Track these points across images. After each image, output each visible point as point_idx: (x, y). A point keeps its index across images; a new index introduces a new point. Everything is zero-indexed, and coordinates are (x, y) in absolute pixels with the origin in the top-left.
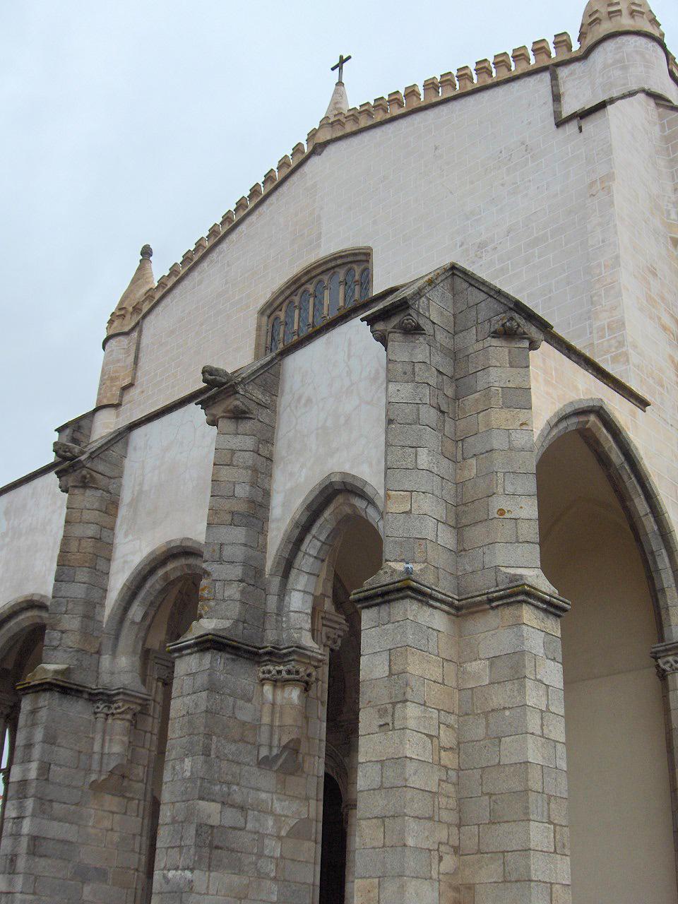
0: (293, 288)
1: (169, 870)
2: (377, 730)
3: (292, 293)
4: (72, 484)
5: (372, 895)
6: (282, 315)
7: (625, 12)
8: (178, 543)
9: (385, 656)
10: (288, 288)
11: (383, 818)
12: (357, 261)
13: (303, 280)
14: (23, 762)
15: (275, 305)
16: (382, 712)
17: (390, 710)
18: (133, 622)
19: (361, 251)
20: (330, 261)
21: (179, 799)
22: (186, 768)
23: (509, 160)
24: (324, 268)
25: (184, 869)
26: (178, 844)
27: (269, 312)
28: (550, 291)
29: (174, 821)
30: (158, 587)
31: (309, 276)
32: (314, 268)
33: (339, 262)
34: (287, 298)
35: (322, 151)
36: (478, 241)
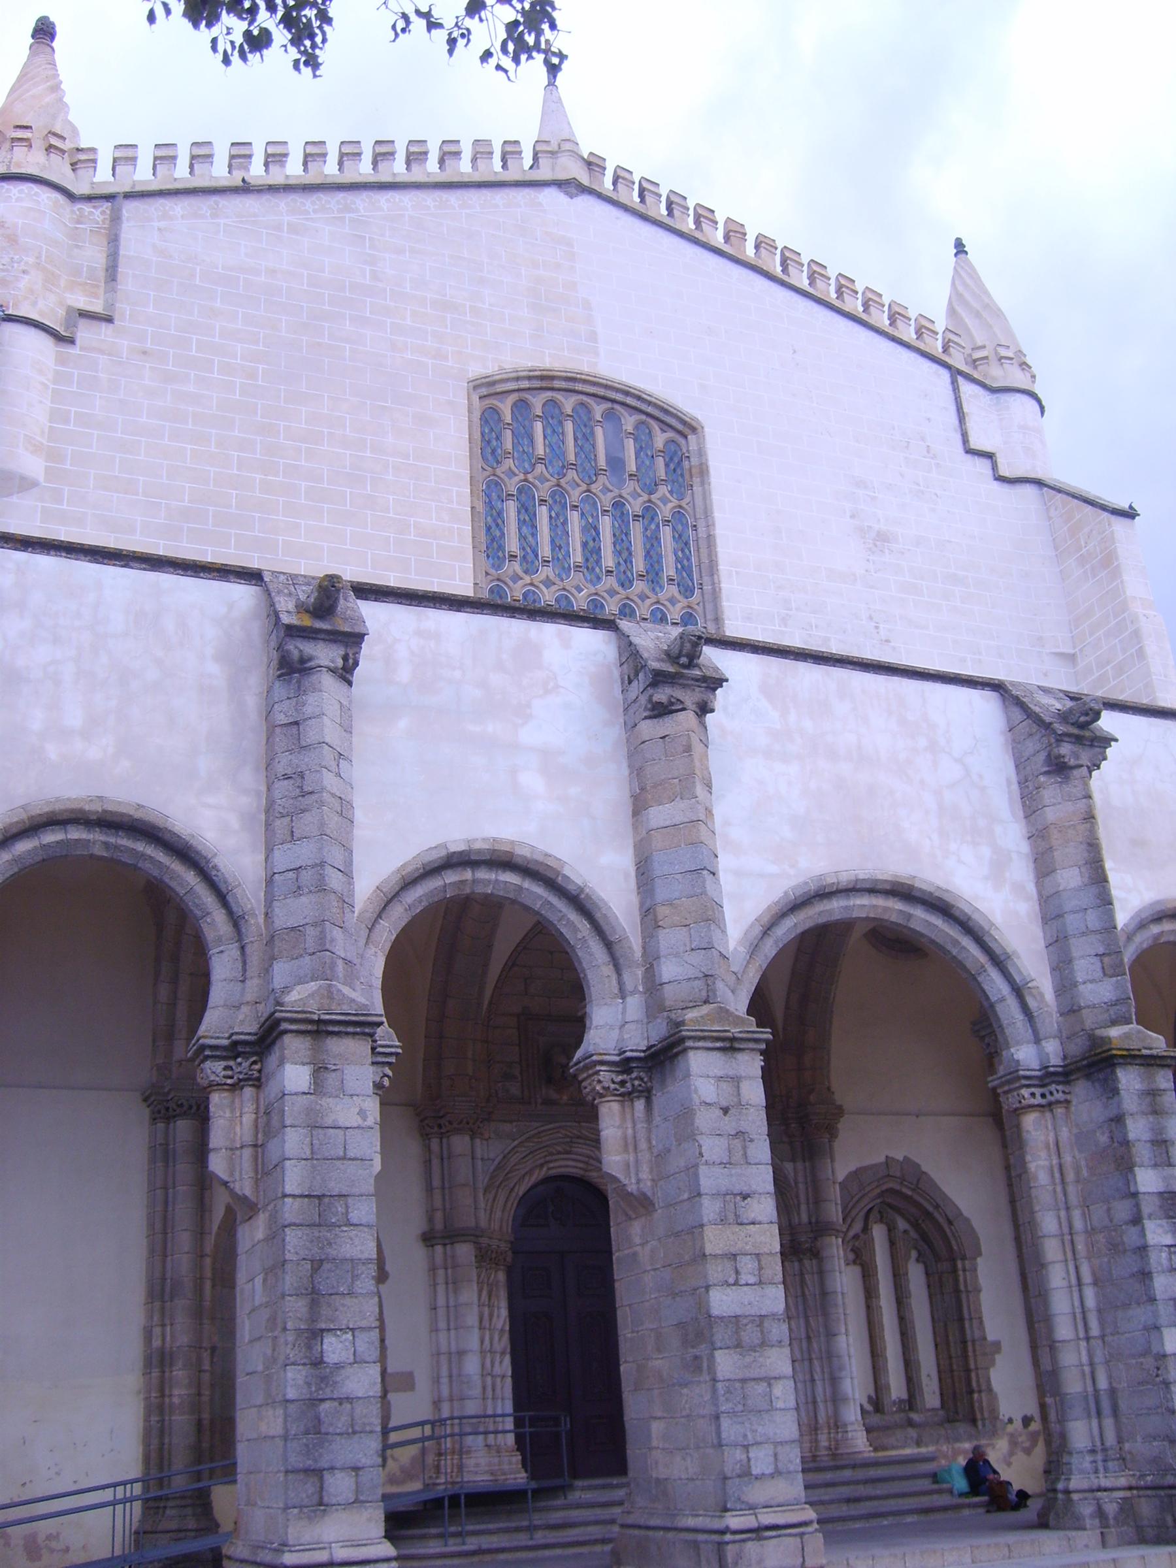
0: (537, 384)
3: (529, 389)
6: (506, 409)
7: (992, 357)
10: (529, 378)
12: (662, 422)
13: (557, 384)
15: (500, 388)
19: (680, 414)
20: (617, 390)
23: (907, 447)
24: (601, 392)
27: (484, 391)
30: (1145, 946)
31: (570, 385)
32: (585, 382)
33: (629, 401)
34: (519, 390)
35: (577, 195)
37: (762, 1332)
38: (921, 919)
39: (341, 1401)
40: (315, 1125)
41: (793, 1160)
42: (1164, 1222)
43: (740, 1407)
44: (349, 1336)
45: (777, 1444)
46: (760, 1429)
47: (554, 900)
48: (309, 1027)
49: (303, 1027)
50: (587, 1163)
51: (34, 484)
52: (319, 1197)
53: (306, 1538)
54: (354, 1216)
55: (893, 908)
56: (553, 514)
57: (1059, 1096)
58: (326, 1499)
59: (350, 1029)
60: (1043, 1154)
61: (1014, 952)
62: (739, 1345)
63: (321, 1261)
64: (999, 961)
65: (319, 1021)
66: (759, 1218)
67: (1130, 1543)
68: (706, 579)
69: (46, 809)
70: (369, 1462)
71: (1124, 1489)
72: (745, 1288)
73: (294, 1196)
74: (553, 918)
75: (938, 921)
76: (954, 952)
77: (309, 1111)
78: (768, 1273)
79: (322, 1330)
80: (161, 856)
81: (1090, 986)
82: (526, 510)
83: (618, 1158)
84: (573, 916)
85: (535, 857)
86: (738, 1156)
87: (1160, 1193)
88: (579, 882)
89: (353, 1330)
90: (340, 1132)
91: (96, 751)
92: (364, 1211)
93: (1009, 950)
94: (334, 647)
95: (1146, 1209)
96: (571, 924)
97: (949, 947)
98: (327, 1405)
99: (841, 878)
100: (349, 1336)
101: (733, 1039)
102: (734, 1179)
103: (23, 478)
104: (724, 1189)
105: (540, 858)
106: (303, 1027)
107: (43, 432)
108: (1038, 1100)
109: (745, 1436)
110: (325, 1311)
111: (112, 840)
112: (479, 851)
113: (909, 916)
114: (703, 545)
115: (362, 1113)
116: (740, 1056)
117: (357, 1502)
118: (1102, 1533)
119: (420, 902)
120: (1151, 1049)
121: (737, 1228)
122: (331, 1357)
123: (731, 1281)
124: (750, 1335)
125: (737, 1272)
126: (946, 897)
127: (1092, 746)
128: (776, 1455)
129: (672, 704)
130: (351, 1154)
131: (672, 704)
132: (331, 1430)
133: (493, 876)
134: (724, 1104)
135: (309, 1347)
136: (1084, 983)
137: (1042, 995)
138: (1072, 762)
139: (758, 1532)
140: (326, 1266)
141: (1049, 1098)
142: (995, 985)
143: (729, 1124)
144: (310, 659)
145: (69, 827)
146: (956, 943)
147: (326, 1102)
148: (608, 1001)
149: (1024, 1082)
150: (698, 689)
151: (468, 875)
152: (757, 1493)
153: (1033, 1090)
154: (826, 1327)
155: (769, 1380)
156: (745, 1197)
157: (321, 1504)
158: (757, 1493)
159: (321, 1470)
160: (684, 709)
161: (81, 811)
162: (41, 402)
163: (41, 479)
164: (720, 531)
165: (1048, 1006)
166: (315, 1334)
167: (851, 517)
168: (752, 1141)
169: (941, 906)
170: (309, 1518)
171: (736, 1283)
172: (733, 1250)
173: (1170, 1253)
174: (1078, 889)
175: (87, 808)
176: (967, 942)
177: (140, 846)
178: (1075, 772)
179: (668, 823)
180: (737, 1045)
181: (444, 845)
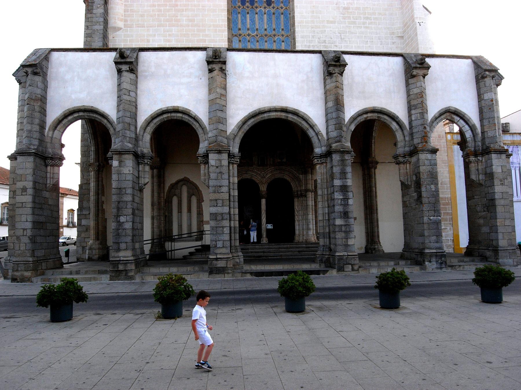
1: (430, 217)
2: (499, 185)
4: (338, 72)
5: (502, 223)
8: (380, 109)
9: (500, 167)
11: (504, 206)
14: (341, 178)
16: (501, 181)
17: (503, 180)
18: (351, 131)
21: (431, 196)
22: (432, 187)
25: (437, 216)
26: (433, 209)
28: (373, 39)
29: (429, 203)
30: (362, 120)
36: (344, 6)
37: (222, 217)
38: (291, 117)
39: (123, 229)
40: (119, 173)
41: (302, 174)
42: (341, 193)
43: (215, 233)
44: (126, 217)
45: (223, 241)
46: (220, 238)
47: (190, 119)
48: (118, 153)
49: (116, 153)
50: (252, 176)
51: (121, 29)
52: (120, 188)
53: (116, 256)
54: (127, 192)
55: (283, 115)
56: (251, 16)
57: (324, 161)
58: (120, 248)
59: (127, 153)
60: (320, 175)
61: (316, 125)
62: (216, 219)
63: (120, 201)
64: (312, 126)
65: (120, 151)
66: (224, 191)
67: (414, 265)
68: (292, 28)
69: (73, 109)
70: (129, 242)
71: (328, 255)
72: (219, 207)
73: (114, 188)
74: (191, 123)
75: (295, 117)
76: (300, 125)
77: (118, 170)
78: (225, 204)
79: (120, 215)
80: (99, 117)
81: (331, 133)
82: (244, 16)
83: (203, 178)
84: (195, 123)
85: (184, 110)
86: (219, 178)
87: (341, 186)
88: (194, 115)
89: (126, 215)
90: (125, 175)
91: (83, 95)
92: (129, 191)
93: (314, 124)
94: (126, 65)
95: (336, 190)
96: (194, 125)
97: (299, 124)
98: (120, 230)
99: (265, 109)
100: (126, 217)
101: (220, 151)
102: (218, 183)
103: (118, 28)
104: (215, 185)
105: (185, 110)
106: (116, 153)
107: (122, 16)
108: (319, 162)
109: (216, 239)
110: (120, 212)
111: (89, 114)
112: (170, 109)
113: (287, 117)
114: (292, 18)
115: (129, 171)
116: (222, 154)
117: (126, 249)
118: (320, 265)
119: (158, 122)
120: (345, 149)
121: (218, 194)
122: (121, 221)
123: (215, 205)
124: (219, 218)
125: (217, 204)
126: (297, 111)
127: (340, 67)
128: (223, 243)
129: (213, 69)
130: (127, 179)
131: (213, 69)
132: (121, 235)
133: (175, 115)
134: (217, 165)
135: (117, 219)
136: (330, 132)
137: (322, 136)
138: (333, 72)
139: (217, 259)
140: (121, 202)
141: (322, 162)
142: (311, 133)
143: (218, 170)
144: (121, 69)
145: (79, 113)
146: (300, 123)
147: (122, 168)
148: (202, 142)
149: (315, 158)
150: (219, 64)
151: (169, 115)
152: (218, 251)
153: (318, 159)
154: (307, 213)
155: (223, 227)
156: (220, 187)
157: (119, 249)
158: (218, 251)
159: (119, 243)
160: (215, 70)
161: (80, 109)
162: (121, 8)
163: (123, 27)
164: (296, 14)
165: (324, 138)
166: (118, 216)
167: (336, 4)
168: (223, 174)
169: (295, 113)
170: (116, 252)
171: (217, 206)
172: (216, 199)
173: (341, 201)
174: (331, 107)
175: (81, 108)
176: (304, 123)
177: (95, 115)
178: (335, 75)
179: (211, 99)
180: (221, 152)
181: (161, 109)
